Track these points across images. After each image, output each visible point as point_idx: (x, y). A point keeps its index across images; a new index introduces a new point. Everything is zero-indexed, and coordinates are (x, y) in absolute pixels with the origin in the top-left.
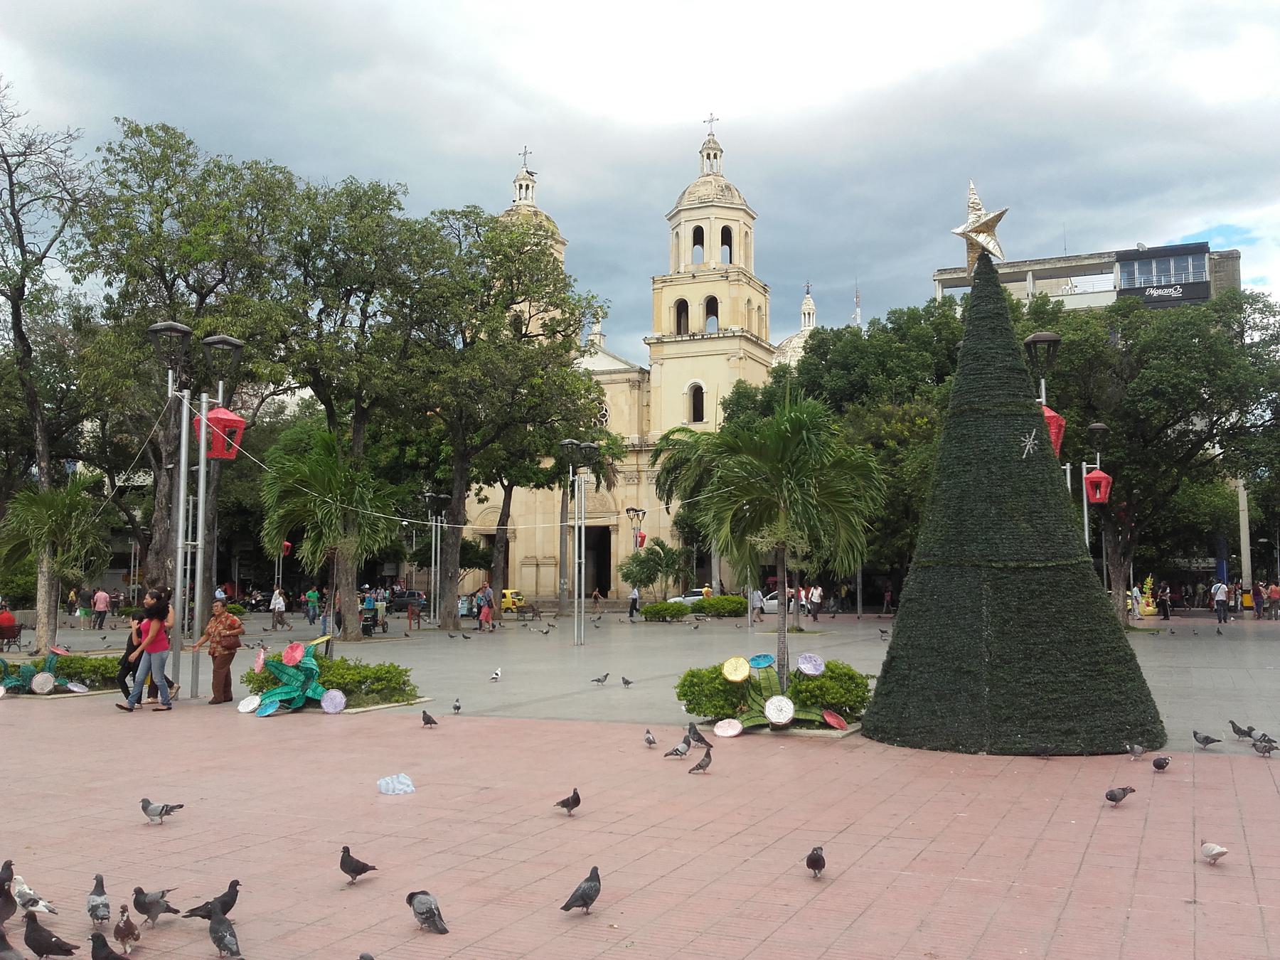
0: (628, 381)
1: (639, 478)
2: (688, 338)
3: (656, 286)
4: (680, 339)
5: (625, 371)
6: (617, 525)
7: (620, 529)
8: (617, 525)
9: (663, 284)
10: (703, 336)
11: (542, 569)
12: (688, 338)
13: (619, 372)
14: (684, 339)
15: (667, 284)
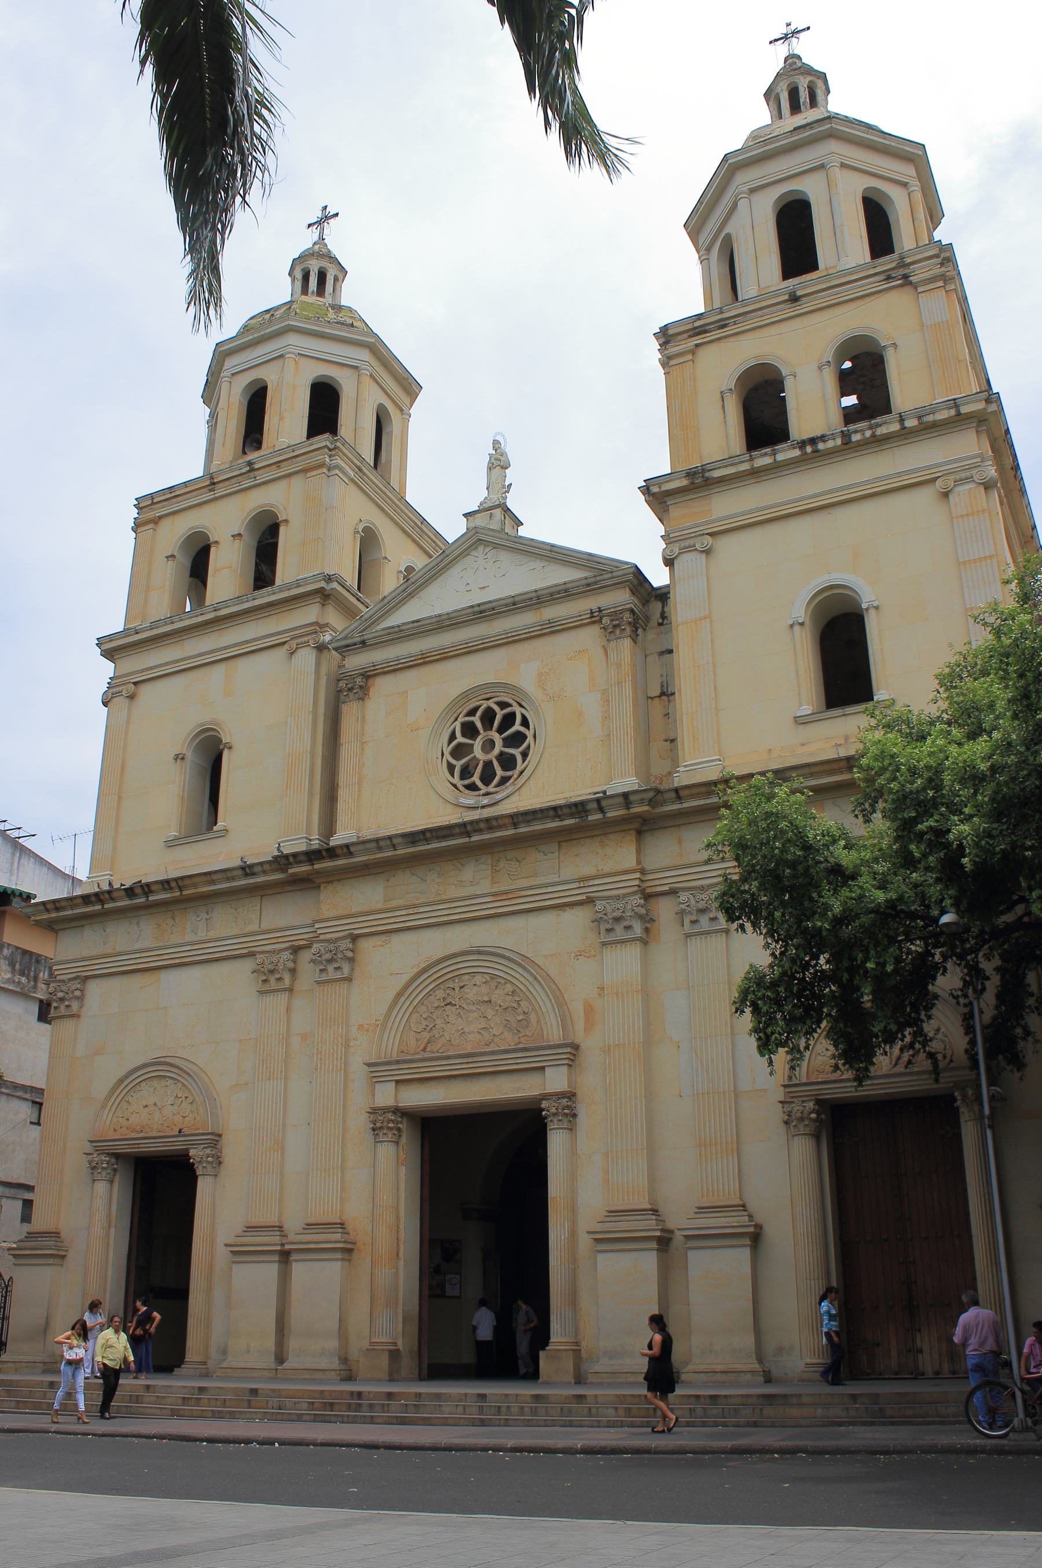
0: (595, 617)
1: (648, 920)
2: (797, 453)
3: (672, 350)
4: (768, 460)
5: (589, 588)
6: (571, 1096)
7: (582, 1110)
8: (571, 1096)
9: (697, 340)
10: (846, 436)
11: (299, 1270)
12: (797, 453)
13: (562, 594)
14: (780, 457)
15: (709, 337)
